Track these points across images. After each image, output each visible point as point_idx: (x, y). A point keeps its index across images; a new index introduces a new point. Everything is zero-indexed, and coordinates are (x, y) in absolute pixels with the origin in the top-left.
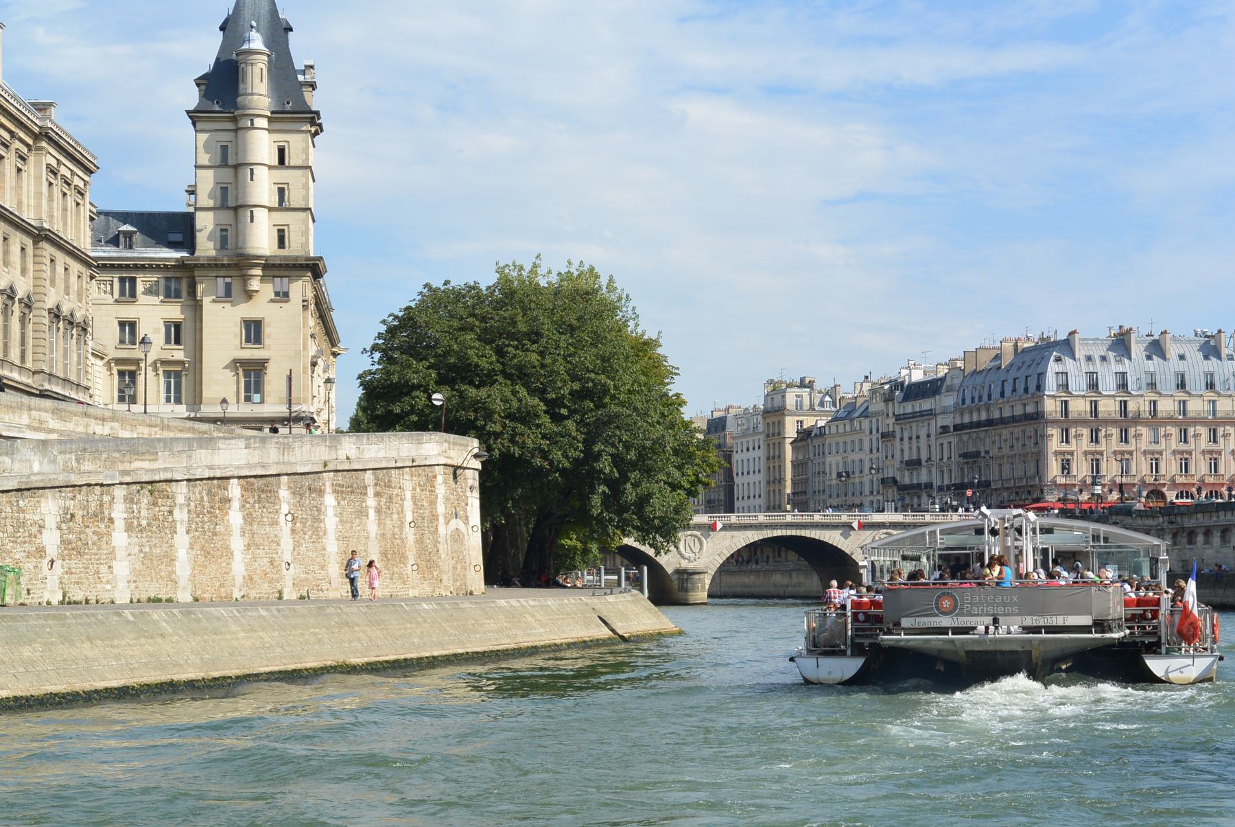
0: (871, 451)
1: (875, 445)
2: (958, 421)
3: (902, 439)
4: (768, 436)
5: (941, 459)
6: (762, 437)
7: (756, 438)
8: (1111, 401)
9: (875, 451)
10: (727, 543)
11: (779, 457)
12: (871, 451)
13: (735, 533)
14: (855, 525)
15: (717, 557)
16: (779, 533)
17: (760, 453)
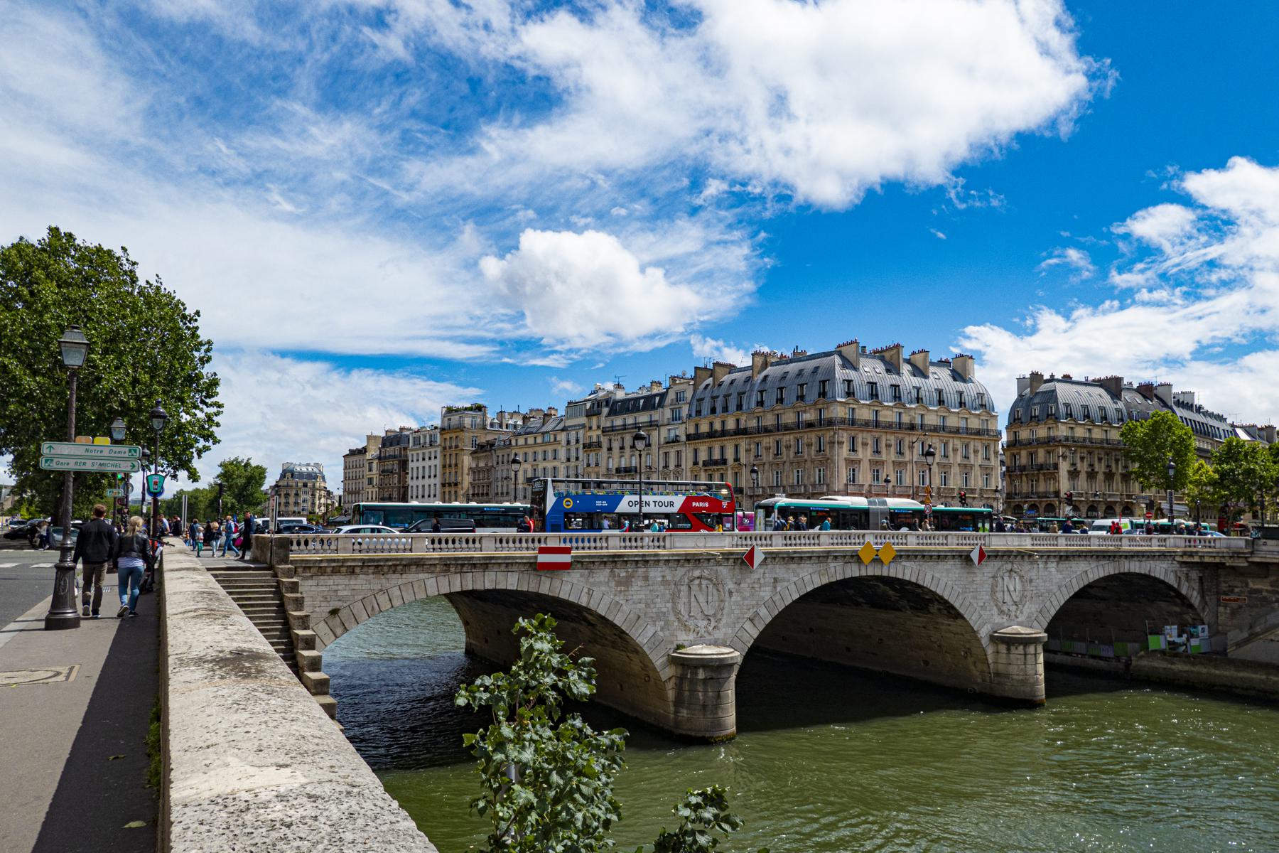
0: (568, 460)
1: (573, 454)
2: (692, 430)
3: (610, 449)
4: (445, 448)
5: (666, 467)
6: (439, 450)
7: (433, 450)
8: (889, 413)
9: (573, 459)
10: (766, 593)
11: (456, 465)
12: (568, 460)
13: (780, 571)
14: (975, 556)
15: (748, 626)
16: (853, 571)
17: (438, 462)
